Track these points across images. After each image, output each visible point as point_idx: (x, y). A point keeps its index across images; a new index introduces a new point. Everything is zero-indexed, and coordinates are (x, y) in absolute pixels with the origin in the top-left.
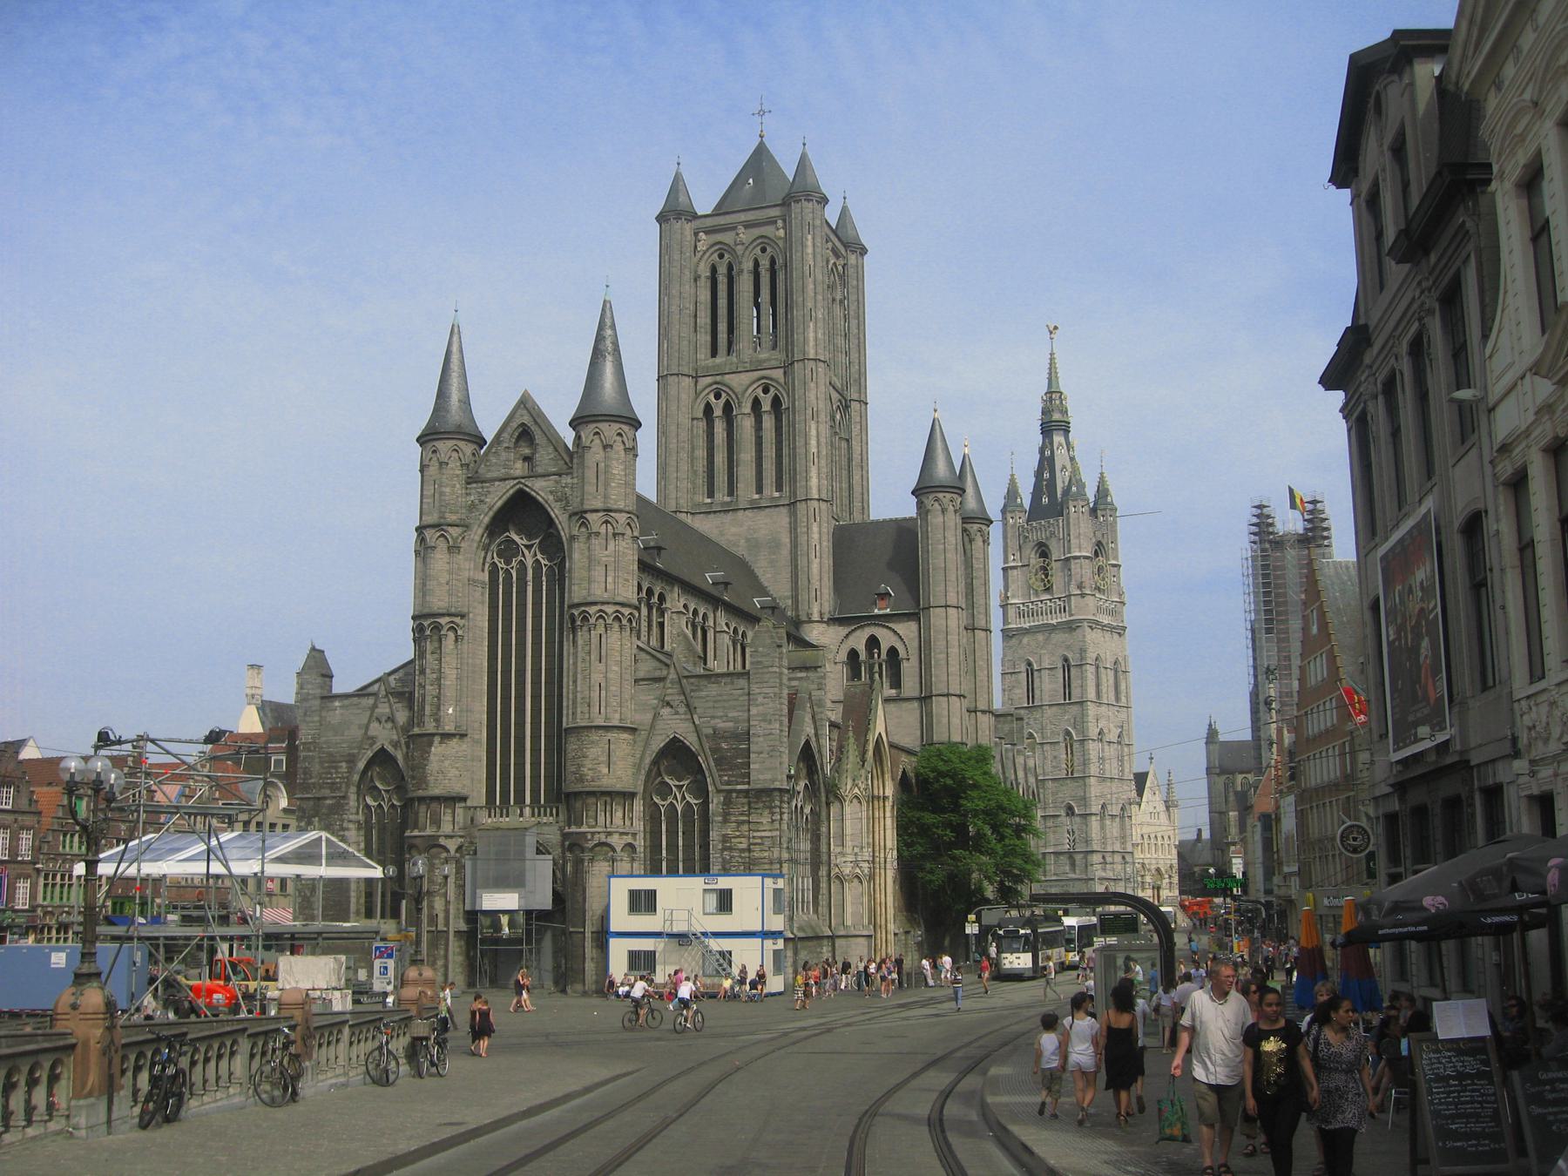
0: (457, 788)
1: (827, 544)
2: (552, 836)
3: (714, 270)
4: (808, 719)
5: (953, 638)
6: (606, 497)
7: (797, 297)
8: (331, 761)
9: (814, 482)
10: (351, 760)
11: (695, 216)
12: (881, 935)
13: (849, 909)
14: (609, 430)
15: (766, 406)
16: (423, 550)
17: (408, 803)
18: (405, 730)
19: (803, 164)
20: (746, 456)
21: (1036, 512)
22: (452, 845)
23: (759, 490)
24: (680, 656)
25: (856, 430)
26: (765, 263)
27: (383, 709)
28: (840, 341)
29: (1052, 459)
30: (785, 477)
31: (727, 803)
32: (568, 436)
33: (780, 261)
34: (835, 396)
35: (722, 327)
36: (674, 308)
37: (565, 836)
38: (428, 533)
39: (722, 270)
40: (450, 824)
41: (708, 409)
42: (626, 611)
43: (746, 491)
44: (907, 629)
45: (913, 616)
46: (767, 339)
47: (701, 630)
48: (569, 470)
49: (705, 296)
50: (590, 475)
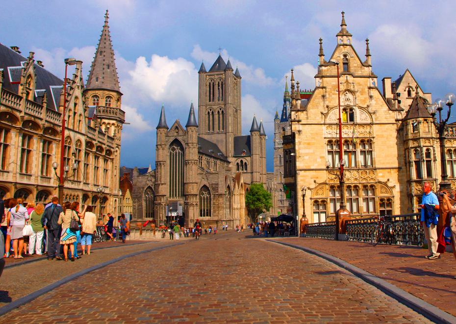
0: (164, 194)
1: (233, 141)
2: (182, 202)
3: (210, 84)
4: (229, 181)
5: (257, 161)
6: (192, 141)
7: (227, 91)
8: (139, 188)
9: (230, 129)
10: (143, 188)
11: (206, 72)
12: (242, 220)
13: (236, 215)
14: (193, 128)
15: (221, 113)
16: (158, 149)
17: (155, 196)
18: (154, 183)
19: (229, 61)
20: (216, 123)
21: (282, 120)
22: (163, 204)
23: (219, 130)
24: (205, 168)
25: (239, 116)
26: (220, 83)
27: (149, 178)
28: (236, 97)
29: (286, 108)
30: (224, 128)
31: (214, 196)
32: (185, 129)
33: (223, 83)
34: (235, 109)
35: (212, 96)
36: (202, 92)
37: (185, 202)
38: (158, 146)
39: (212, 84)
40: (163, 200)
41: (209, 113)
42: (196, 162)
43: (216, 129)
44: (248, 159)
45: (250, 156)
46: (221, 99)
47: (208, 162)
48: (185, 135)
49: (208, 89)
50: (189, 136)
